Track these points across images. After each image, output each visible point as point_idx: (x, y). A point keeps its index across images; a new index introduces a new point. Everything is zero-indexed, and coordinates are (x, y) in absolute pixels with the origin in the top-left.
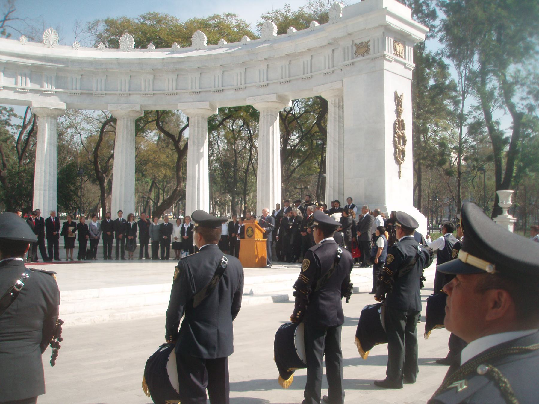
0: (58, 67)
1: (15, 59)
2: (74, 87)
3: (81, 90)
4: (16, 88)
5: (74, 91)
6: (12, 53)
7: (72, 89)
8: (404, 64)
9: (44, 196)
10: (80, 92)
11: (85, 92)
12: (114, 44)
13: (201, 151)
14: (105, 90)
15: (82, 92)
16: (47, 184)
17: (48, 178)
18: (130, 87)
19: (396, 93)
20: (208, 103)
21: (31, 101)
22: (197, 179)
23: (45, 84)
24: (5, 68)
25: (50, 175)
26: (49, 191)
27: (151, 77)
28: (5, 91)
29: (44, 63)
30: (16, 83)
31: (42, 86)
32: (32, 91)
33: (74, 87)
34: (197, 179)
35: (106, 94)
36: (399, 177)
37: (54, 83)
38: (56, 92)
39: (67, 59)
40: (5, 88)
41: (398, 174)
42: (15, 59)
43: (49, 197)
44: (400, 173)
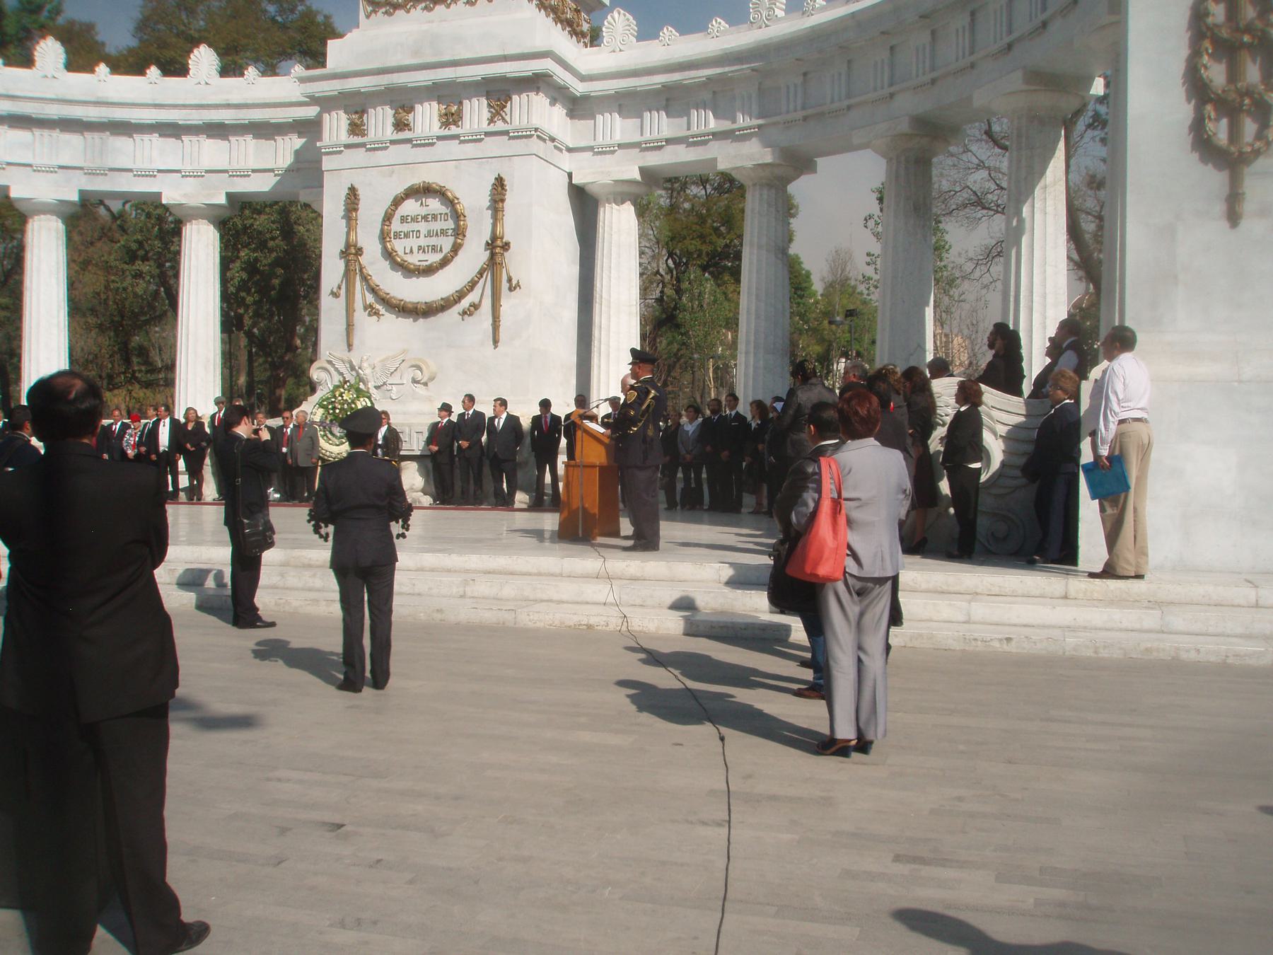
0: (753, 70)
1: (676, 77)
2: (791, 107)
3: (803, 108)
4: (687, 137)
5: (789, 117)
6: (669, 65)
7: (788, 112)
9: (747, 367)
10: (800, 115)
11: (810, 112)
12: (175, 68)
13: (1026, 210)
14: (849, 96)
15: (804, 113)
16: (752, 338)
17: (753, 326)
18: (892, 76)
20: (1019, 75)
21: (715, 159)
22: (1012, 299)
23: (740, 117)
24: (667, 100)
25: (758, 317)
26: (755, 354)
27: (925, 37)
28: (670, 148)
29: (727, 69)
30: (689, 129)
31: (734, 121)
32: (717, 135)
33: (791, 107)
34: (1012, 299)
35: (849, 108)
37: (755, 107)
38: (759, 127)
39: (765, 45)
40: (669, 141)
42: (676, 77)
43: (755, 368)
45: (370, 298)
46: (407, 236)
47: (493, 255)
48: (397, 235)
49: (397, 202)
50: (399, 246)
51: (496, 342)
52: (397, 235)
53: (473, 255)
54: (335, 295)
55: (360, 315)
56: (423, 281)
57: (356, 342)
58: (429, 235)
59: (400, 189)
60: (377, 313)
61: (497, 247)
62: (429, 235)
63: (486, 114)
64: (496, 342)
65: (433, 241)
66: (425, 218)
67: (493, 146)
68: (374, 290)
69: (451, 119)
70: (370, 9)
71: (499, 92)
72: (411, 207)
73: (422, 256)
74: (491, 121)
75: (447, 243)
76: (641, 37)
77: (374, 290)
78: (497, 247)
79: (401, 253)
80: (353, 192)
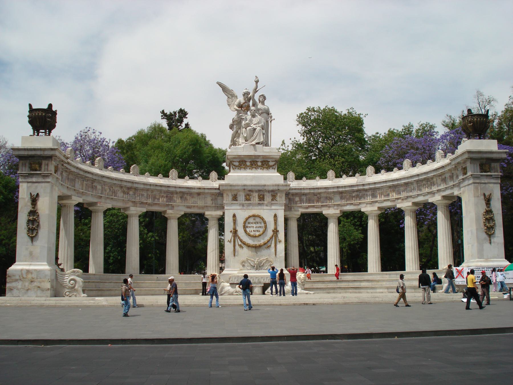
8: (492, 175)
19: (484, 195)
36: (490, 243)
41: (489, 241)
44: (490, 240)
45: (240, 243)
46: (250, 227)
47: (274, 233)
48: (247, 227)
49: (247, 219)
50: (248, 230)
51: (276, 254)
52: (247, 227)
53: (270, 233)
54: (230, 242)
55: (237, 247)
56: (255, 239)
57: (236, 254)
58: (256, 227)
59: (247, 216)
60: (242, 247)
61: (276, 232)
62: (256, 227)
63: (270, 198)
64: (276, 254)
65: (257, 229)
66: (255, 223)
67: (273, 207)
68: (241, 241)
69: (262, 198)
70: (234, 167)
71: (274, 193)
72: (251, 220)
73: (254, 233)
74: (272, 200)
75: (261, 230)
76: (297, 178)
77: (241, 241)
78: (276, 232)
79: (248, 231)
80: (234, 216)
